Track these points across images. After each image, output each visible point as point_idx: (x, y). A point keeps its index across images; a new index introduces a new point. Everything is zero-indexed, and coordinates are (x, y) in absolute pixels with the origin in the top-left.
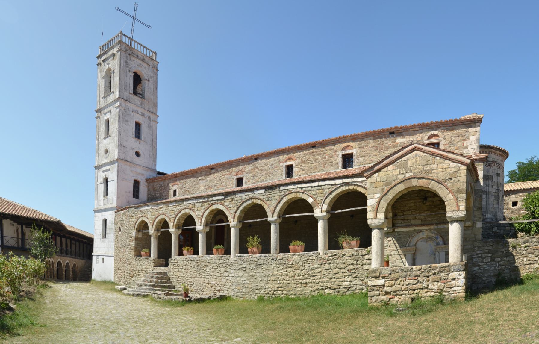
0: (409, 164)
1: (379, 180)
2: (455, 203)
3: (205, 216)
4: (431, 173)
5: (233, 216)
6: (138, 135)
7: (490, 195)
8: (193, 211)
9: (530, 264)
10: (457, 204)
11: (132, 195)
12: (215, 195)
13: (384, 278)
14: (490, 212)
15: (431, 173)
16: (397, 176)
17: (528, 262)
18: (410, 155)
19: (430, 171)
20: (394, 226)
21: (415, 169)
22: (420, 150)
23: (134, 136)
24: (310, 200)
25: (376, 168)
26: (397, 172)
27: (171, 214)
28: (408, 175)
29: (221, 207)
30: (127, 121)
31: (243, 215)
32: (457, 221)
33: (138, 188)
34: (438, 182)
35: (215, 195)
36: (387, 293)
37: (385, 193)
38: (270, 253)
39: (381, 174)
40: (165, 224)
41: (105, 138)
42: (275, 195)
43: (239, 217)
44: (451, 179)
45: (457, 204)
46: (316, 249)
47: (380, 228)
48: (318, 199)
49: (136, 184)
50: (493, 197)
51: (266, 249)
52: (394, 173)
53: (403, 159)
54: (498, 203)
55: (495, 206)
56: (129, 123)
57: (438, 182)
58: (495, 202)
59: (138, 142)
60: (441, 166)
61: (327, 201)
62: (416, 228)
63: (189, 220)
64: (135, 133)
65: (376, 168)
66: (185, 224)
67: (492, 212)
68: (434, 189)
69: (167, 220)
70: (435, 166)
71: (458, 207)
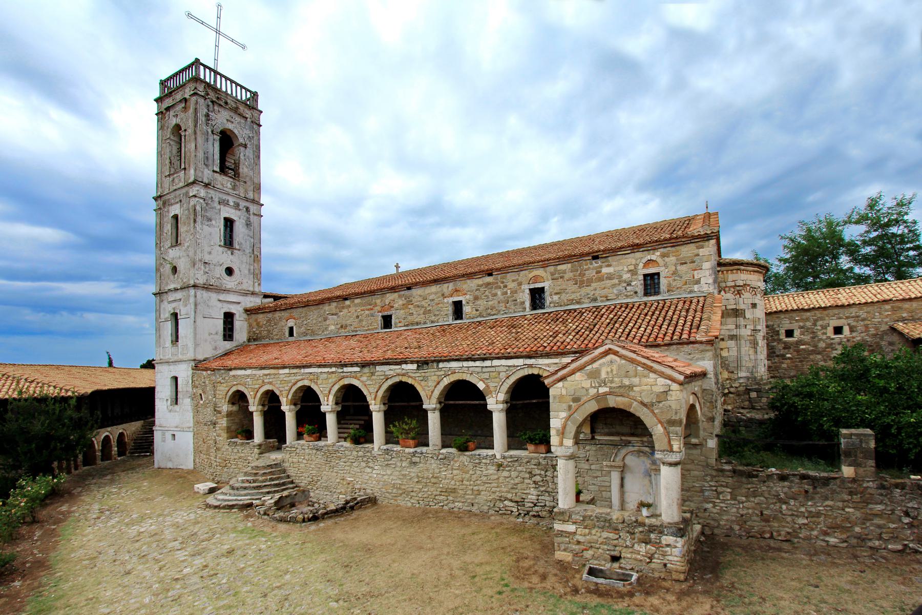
1: (564, 392)
2: (666, 440)
5: (373, 396)
6: (229, 242)
7: (743, 342)
9: (793, 515)
11: (221, 337)
14: (744, 368)
17: (790, 513)
21: (612, 382)
23: (222, 243)
25: (560, 374)
28: (602, 390)
30: (210, 220)
31: (388, 394)
33: (232, 323)
34: (642, 403)
37: (572, 411)
41: (172, 246)
42: (432, 373)
43: (383, 397)
44: (659, 402)
49: (229, 318)
50: (748, 343)
54: (756, 352)
55: (752, 357)
56: (213, 222)
58: (752, 352)
59: (229, 252)
64: (225, 237)
65: (560, 374)
67: (748, 368)
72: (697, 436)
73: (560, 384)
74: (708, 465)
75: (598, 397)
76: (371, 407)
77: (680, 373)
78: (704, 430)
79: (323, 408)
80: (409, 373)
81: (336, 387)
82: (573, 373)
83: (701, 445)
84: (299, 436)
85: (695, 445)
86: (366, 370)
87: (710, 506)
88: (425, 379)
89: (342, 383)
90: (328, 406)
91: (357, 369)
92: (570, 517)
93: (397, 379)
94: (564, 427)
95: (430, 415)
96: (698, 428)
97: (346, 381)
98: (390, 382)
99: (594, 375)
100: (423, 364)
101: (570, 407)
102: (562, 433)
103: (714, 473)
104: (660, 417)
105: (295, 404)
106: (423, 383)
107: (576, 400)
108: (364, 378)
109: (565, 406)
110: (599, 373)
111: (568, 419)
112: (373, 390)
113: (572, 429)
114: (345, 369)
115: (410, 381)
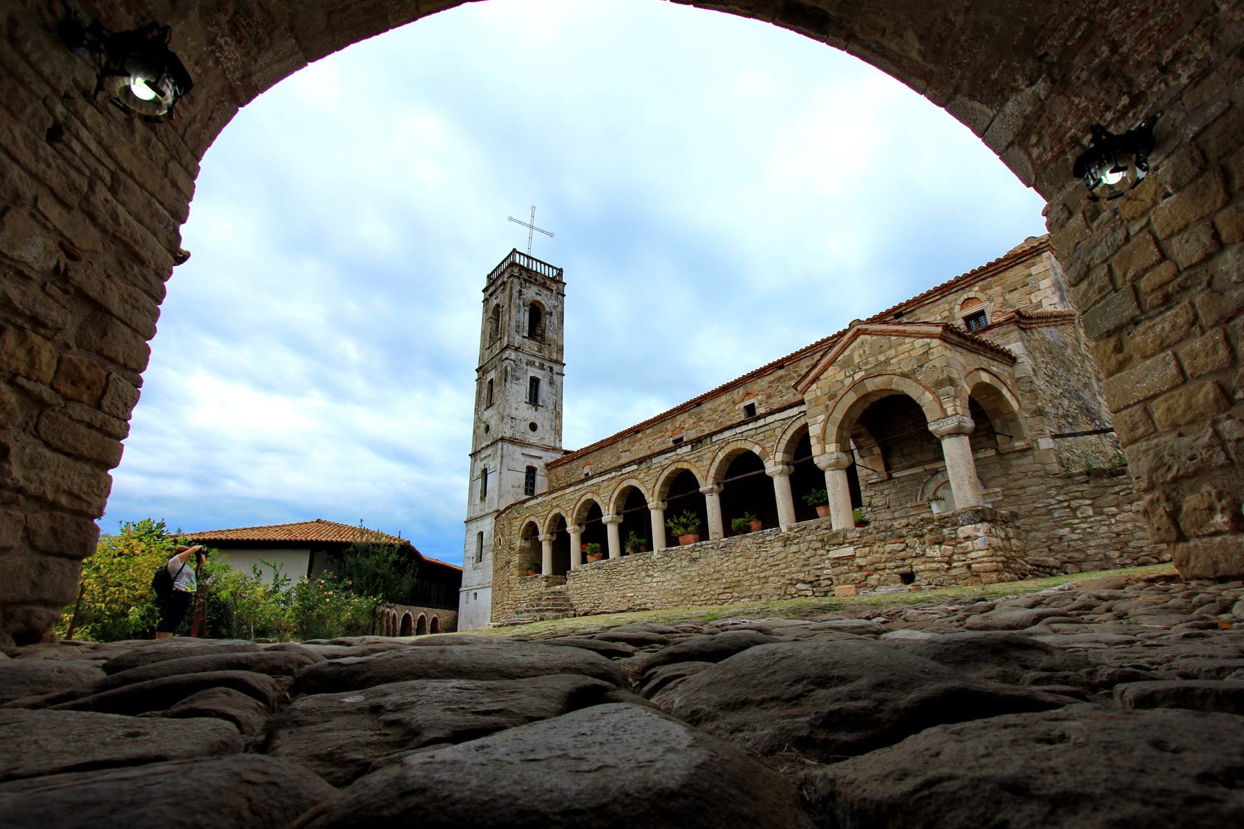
0: (857, 360)
3: (613, 499)
4: (890, 364)
8: (598, 494)
10: (942, 407)
12: (624, 466)
13: (851, 543)
15: (890, 364)
16: (842, 382)
18: (854, 344)
19: (887, 362)
20: (888, 468)
21: (867, 363)
22: (865, 332)
24: (757, 450)
25: (812, 375)
26: (840, 376)
27: (569, 505)
28: (857, 377)
29: (634, 483)
32: (957, 432)
34: (903, 375)
35: (624, 466)
36: (860, 568)
38: (707, 538)
39: (820, 383)
40: (559, 523)
44: (921, 366)
45: (942, 407)
46: (775, 523)
47: (836, 466)
48: (767, 445)
51: (703, 534)
52: (838, 378)
53: (847, 353)
57: (903, 375)
60: (901, 348)
61: (782, 446)
62: (928, 467)
63: (592, 512)
65: (812, 375)
66: (588, 518)
68: (900, 389)
69: (564, 514)
70: (892, 352)
71: (944, 410)
72: (1022, 438)
73: (814, 386)
74: (1047, 474)
75: (853, 386)
76: (649, 506)
77: (937, 325)
78: (1031, 428)
79: (605, 519)
80: (685, 458)
81: (616, 493)
82: (825, 369)
83: (1028, 450)
84: (584, 561)
85: (1023, 451)
86: (643, 466)
87: (1066, 530)
88: (700, 459)
89: (621, 487)
90: (609, 515)
91: (635, 467)
92: (845, 537)
93: (672, 468)
94: (824, 431)
95: (708, 499)
96: (1019, 426)
97: (625, 484)
98: (666, 473)
99: (847, 364)
100: (697, 442)
101: (827, 407)
102: (823, 439)
103: (1059, 482)
104: (924, 382)
105: (580, 525)
106: (698, 464)
107: (832, 397)
108: (642, 476)
109: (822, 408)
110: (852, 360)
111: (826, 421)
112: (650, 486)
113: (833, 431)
114: (624, 471)
115: (685, 466)
